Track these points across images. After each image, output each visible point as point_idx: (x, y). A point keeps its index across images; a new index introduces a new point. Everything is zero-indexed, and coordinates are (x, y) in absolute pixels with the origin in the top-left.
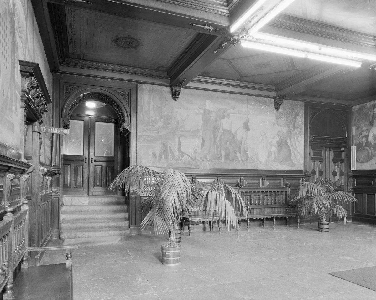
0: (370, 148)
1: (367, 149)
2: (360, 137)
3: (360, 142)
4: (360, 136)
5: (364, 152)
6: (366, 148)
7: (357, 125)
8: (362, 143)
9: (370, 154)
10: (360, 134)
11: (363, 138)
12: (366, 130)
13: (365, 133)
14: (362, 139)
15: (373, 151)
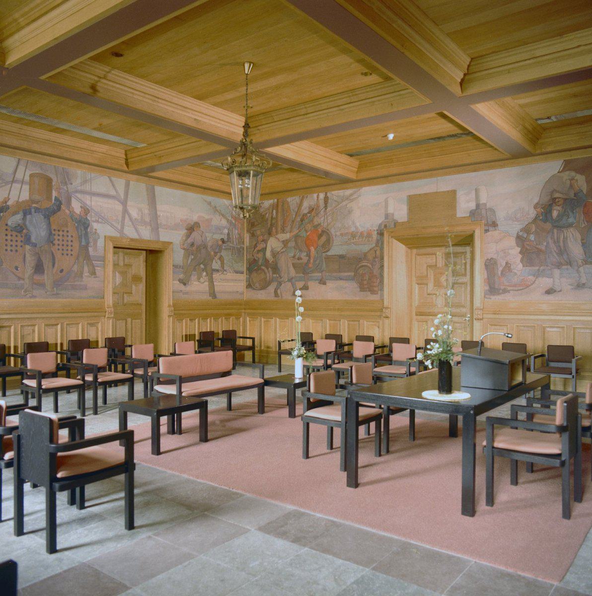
0: (268, 269)
1: (263, 270)
2: (255, 250)
3: (256, 258)
4: (255, 249)
5: (260, 274)
6: (263, 268)
7: (252, 232)
8: (257, 259)
9: (268, 278)
10: (256, 246)
11: (259, 251)
12: (263, 241)
13: (262, 246)
14: (258, 253)
15: (271, 274)
